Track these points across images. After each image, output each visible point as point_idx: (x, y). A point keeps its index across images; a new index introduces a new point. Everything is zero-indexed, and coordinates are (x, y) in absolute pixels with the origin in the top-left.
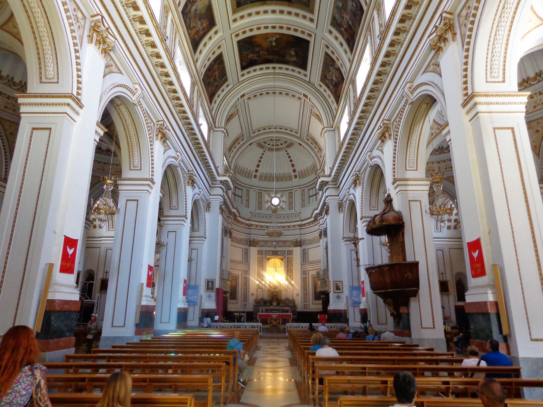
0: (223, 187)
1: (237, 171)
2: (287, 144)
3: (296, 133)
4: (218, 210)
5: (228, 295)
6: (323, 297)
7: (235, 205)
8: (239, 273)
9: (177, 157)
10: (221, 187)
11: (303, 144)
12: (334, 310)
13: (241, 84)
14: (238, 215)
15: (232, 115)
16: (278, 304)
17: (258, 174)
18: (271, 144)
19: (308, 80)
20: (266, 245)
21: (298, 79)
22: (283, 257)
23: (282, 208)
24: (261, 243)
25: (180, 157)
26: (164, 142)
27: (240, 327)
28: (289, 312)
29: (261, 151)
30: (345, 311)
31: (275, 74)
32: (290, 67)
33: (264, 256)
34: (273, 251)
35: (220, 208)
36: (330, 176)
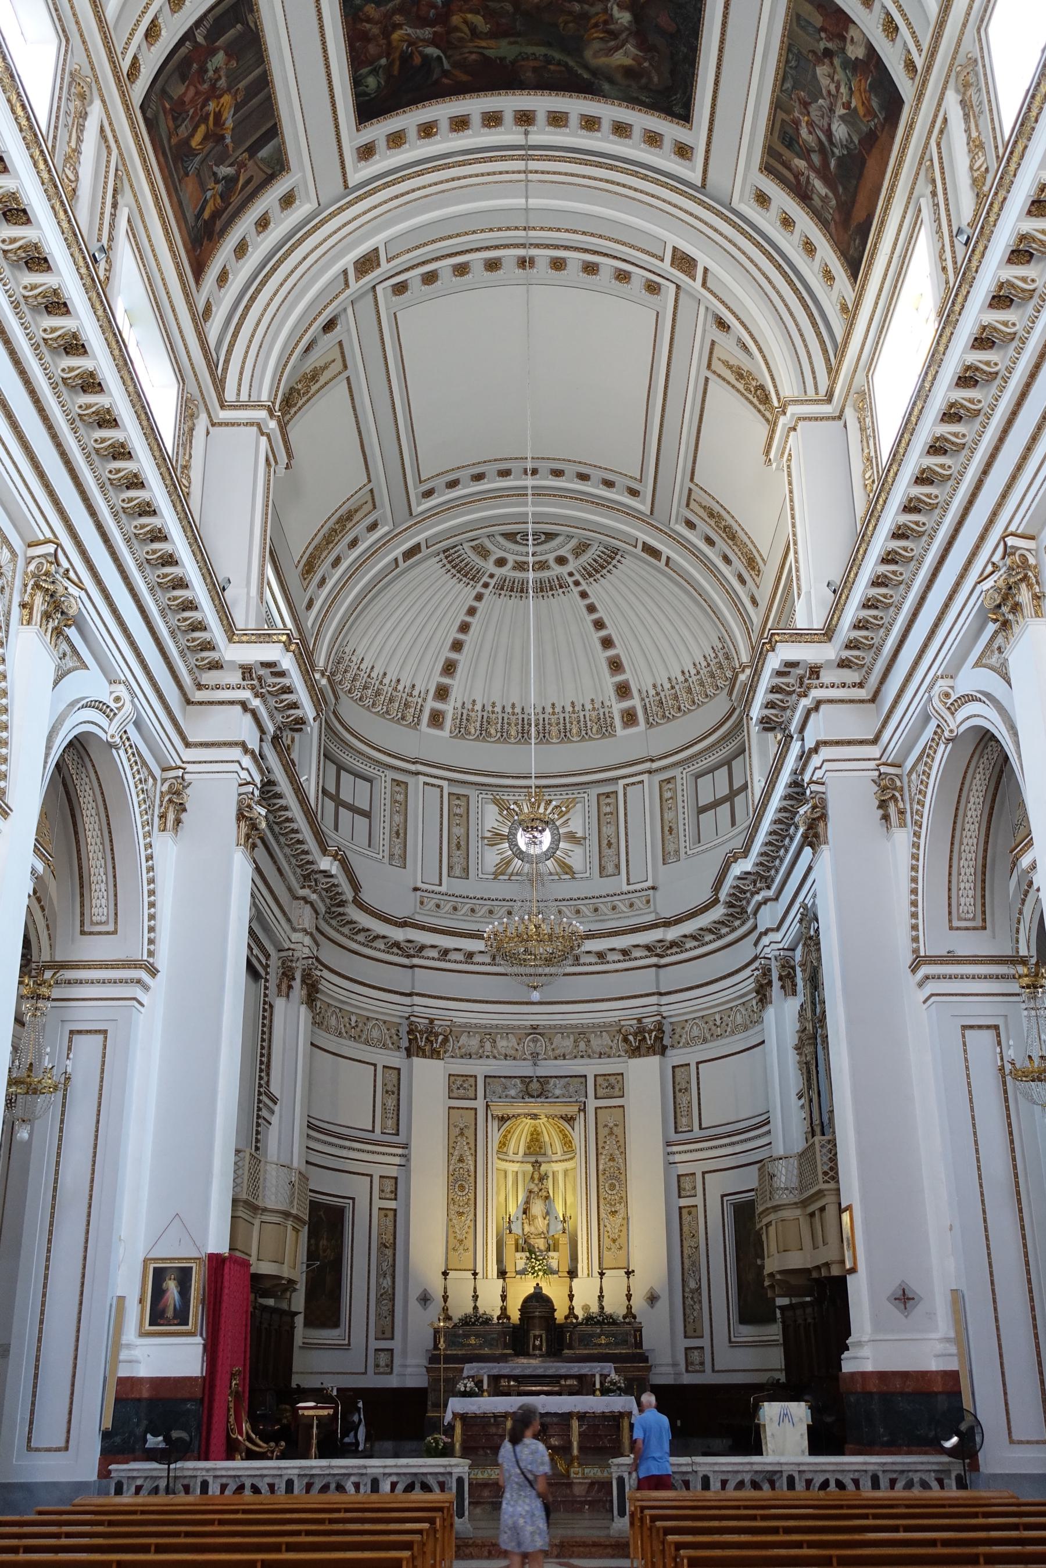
0: (256, 703)
1: (347, 685)
2: (587, 558)
3: (634, 493)
4: (230, 829)
5: (298, 1302)
6: (782, 1308)
7: (334, 839)
8: (358, 1188)
9: (113, 705)
10: (244, 704)
11: (666, 550)
12: (883, 1376)
13: (359, 199)
14: (349, 895)
15: (314, 376)
17: (448, 708)
18: (511, 559)
19: (695, 177)
20: (488, 1046)
21: (645, 178)
24: (464, 1039)
25: (128, 706)
26: (58, 632)
27: (340, 1488)
29: (466, 594)
30: (953, 1376)
31: (527, 152)
32: (609, 111)
34: (526, 1080)
35: (240, 816)
36: (828, 633)
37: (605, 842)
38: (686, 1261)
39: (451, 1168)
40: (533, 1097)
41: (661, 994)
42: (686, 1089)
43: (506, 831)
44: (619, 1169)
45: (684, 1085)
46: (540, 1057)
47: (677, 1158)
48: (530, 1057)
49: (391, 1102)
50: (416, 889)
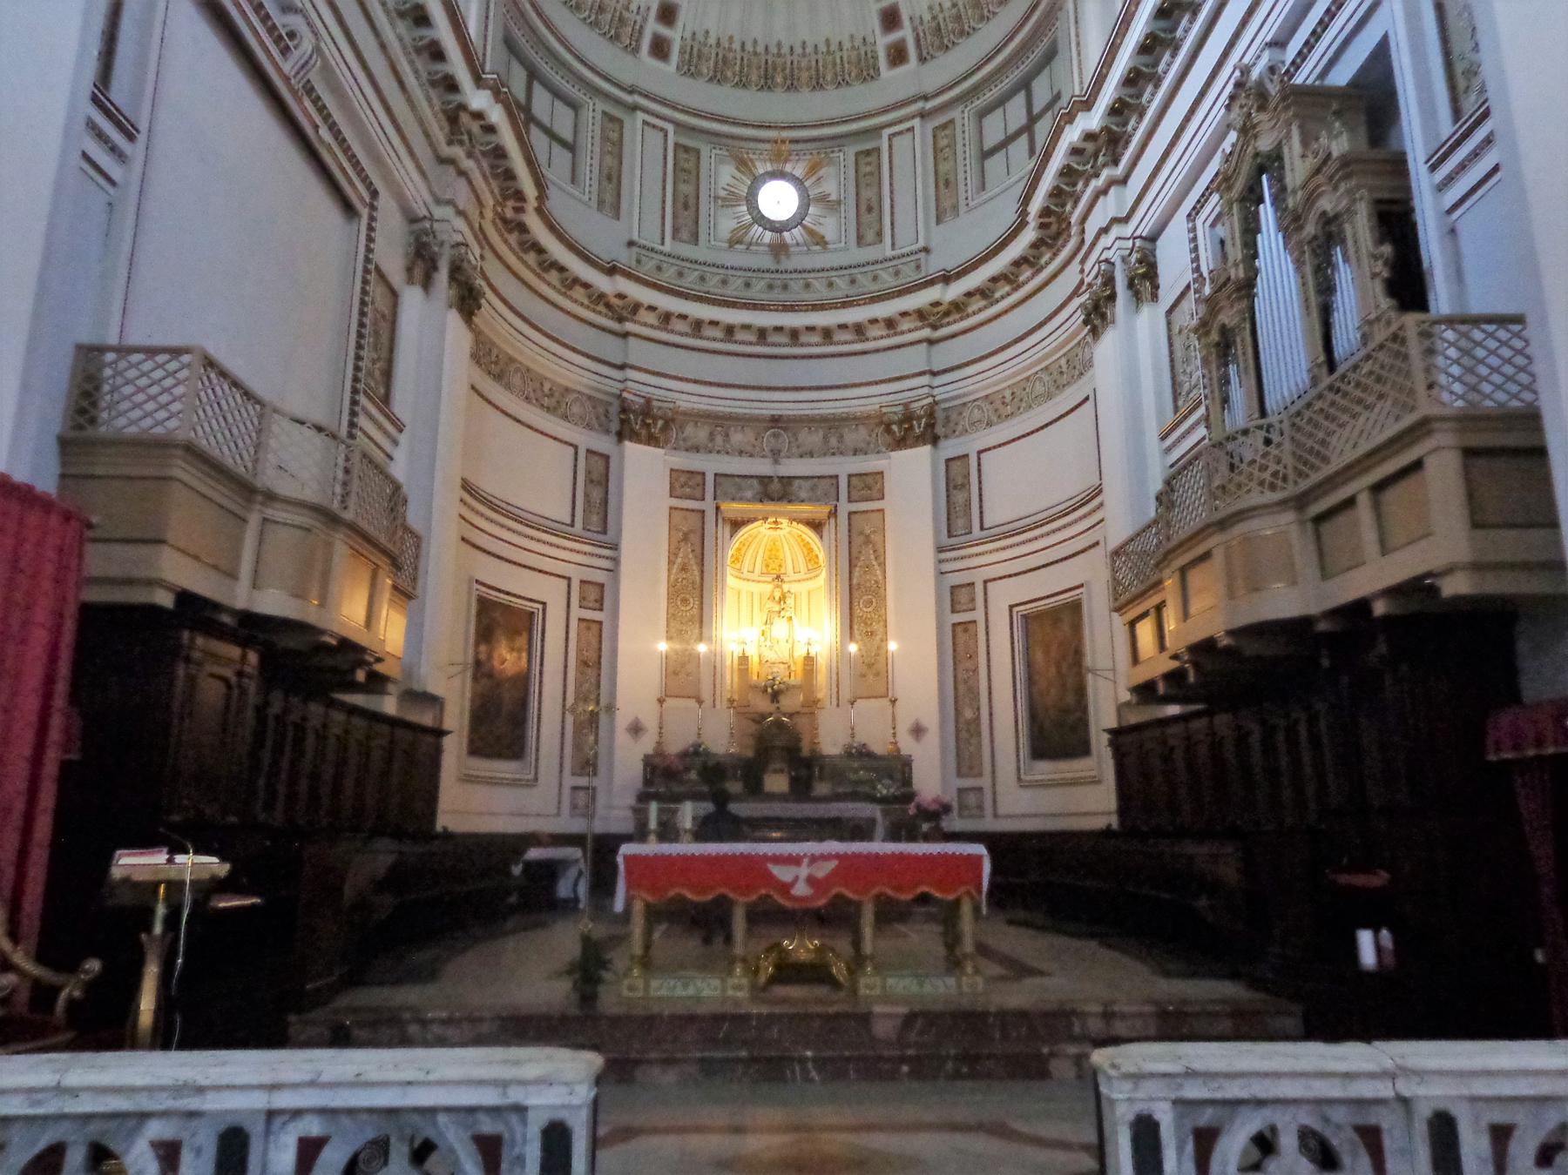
8: (550, 592)
16: (801, 789)
20: (719, 440)
22: (819, 511)
23: (821, 241)
24: (689, 430)
28: (880, 830)
33: (708, 505)
34: (765, 480)
37: (863, 208)
38: (962, 688)
41: (934, 374)
42: (963, 486)
43: (743, 191)
44: (876, 582)
45: (960, 481)
46: (782, 454)
47: (947, 567)
48: (769, 454)
49: (596, 494)
50: (631, 244)
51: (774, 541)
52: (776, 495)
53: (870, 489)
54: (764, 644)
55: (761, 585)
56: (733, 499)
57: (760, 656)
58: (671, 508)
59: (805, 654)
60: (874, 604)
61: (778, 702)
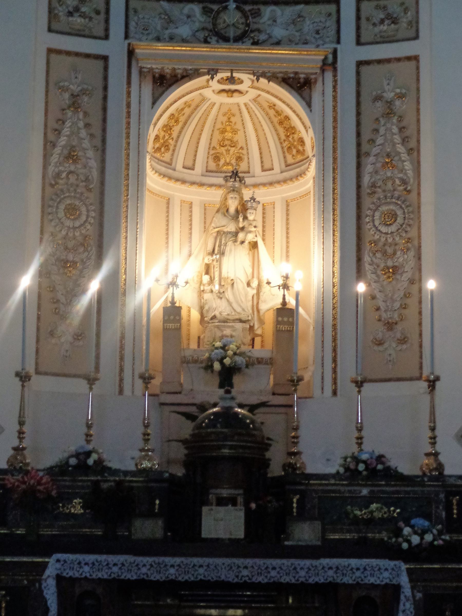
39: (51, 169)
40: (226, 39)
44: (404, 182)
51: (229, 115)
52: (231, 33)
53: (395, 21)
54: (207, 288)
55: (203, 190)
56: (158, 39)
57: (201, 309)
58: (50, 51)
59: (277, 303)
60: (400, 220)
61: (231, 385)
